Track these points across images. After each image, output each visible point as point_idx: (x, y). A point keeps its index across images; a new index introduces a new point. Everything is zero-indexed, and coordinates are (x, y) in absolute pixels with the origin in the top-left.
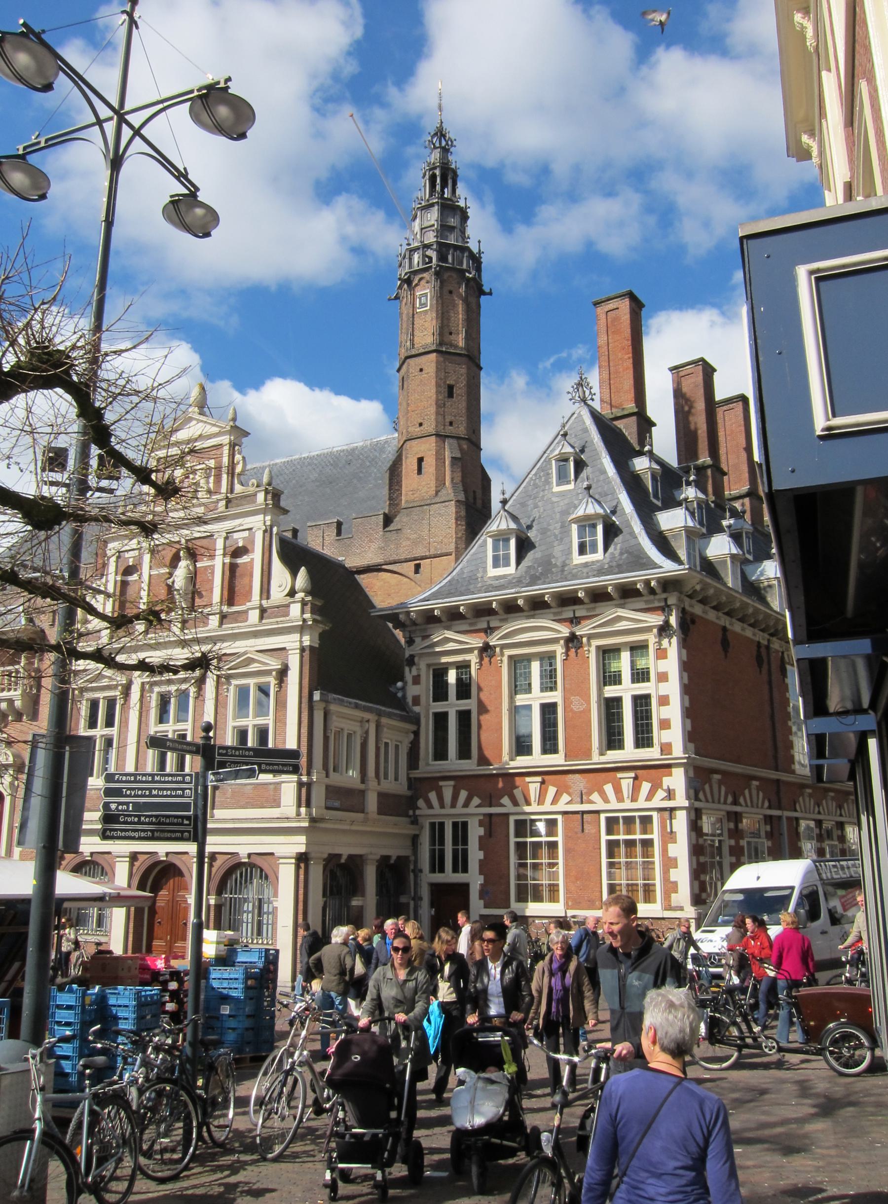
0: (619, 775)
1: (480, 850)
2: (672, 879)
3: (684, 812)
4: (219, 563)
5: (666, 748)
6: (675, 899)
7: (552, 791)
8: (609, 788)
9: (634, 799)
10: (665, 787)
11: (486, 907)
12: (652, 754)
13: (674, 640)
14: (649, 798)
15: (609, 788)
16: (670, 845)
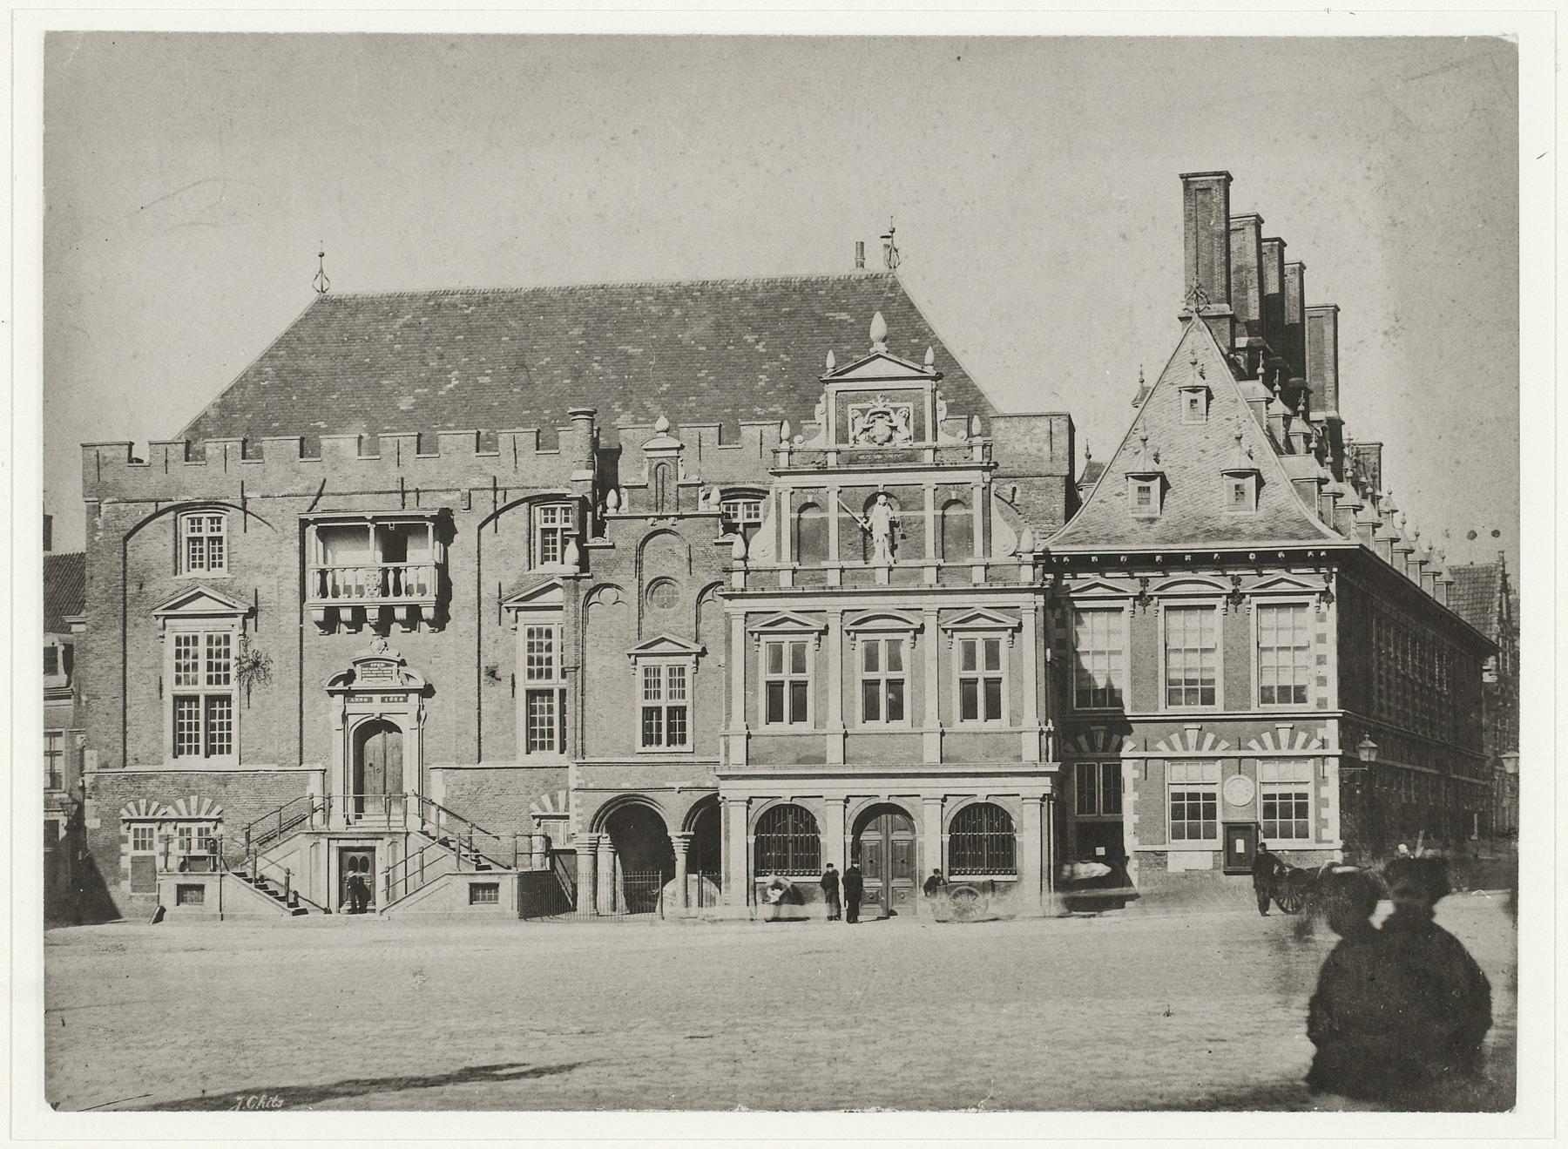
0: (1278, 726)
1: (1135, 790)
2: (1323, 817)
3: (1337, 760)
4: (930, 513)
5: (1322, 703)
6: (1326, 834)
7: (1210, 738)
8: (1267, 737)
9: (1291, 745)
10: (1320, 737)
11: (1141, 843)
12: (1310, 706)
13: (1334, 605)
14: (1304, 747)
15: (1267, 737)
16: (1323, 789)
